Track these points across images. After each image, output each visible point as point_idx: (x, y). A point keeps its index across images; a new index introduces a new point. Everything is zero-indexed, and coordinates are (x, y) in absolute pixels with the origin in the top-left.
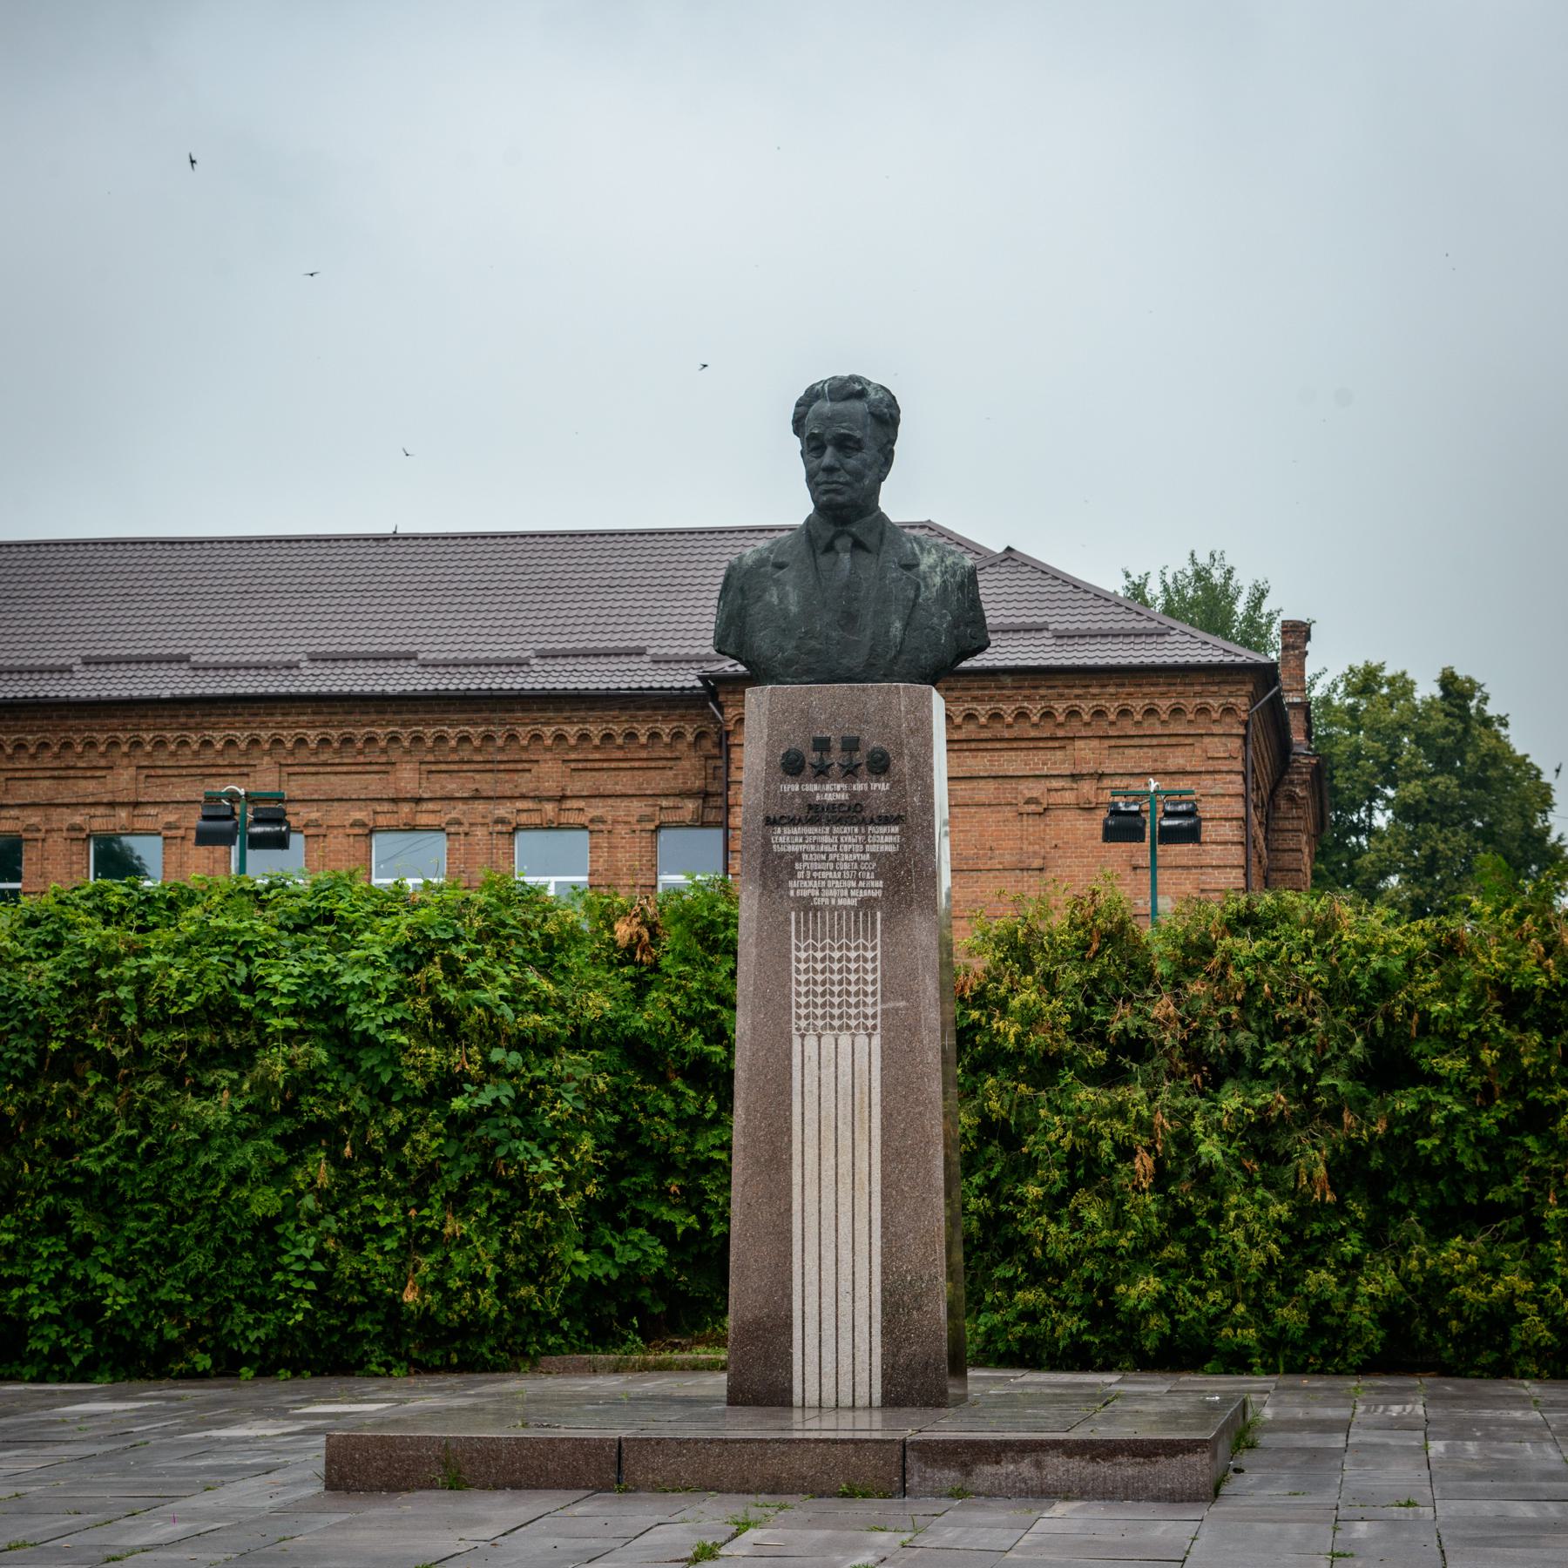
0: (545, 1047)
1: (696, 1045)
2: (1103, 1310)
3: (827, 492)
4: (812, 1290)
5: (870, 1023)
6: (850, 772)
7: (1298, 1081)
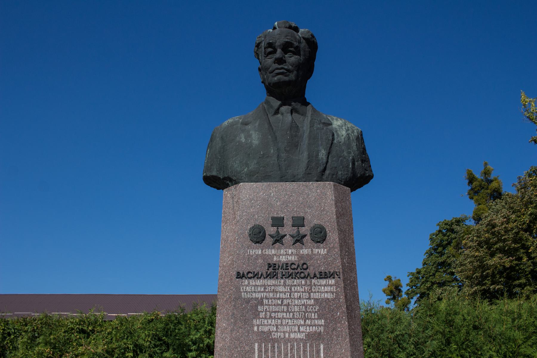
3: (278, 74)
6: (299, 240)
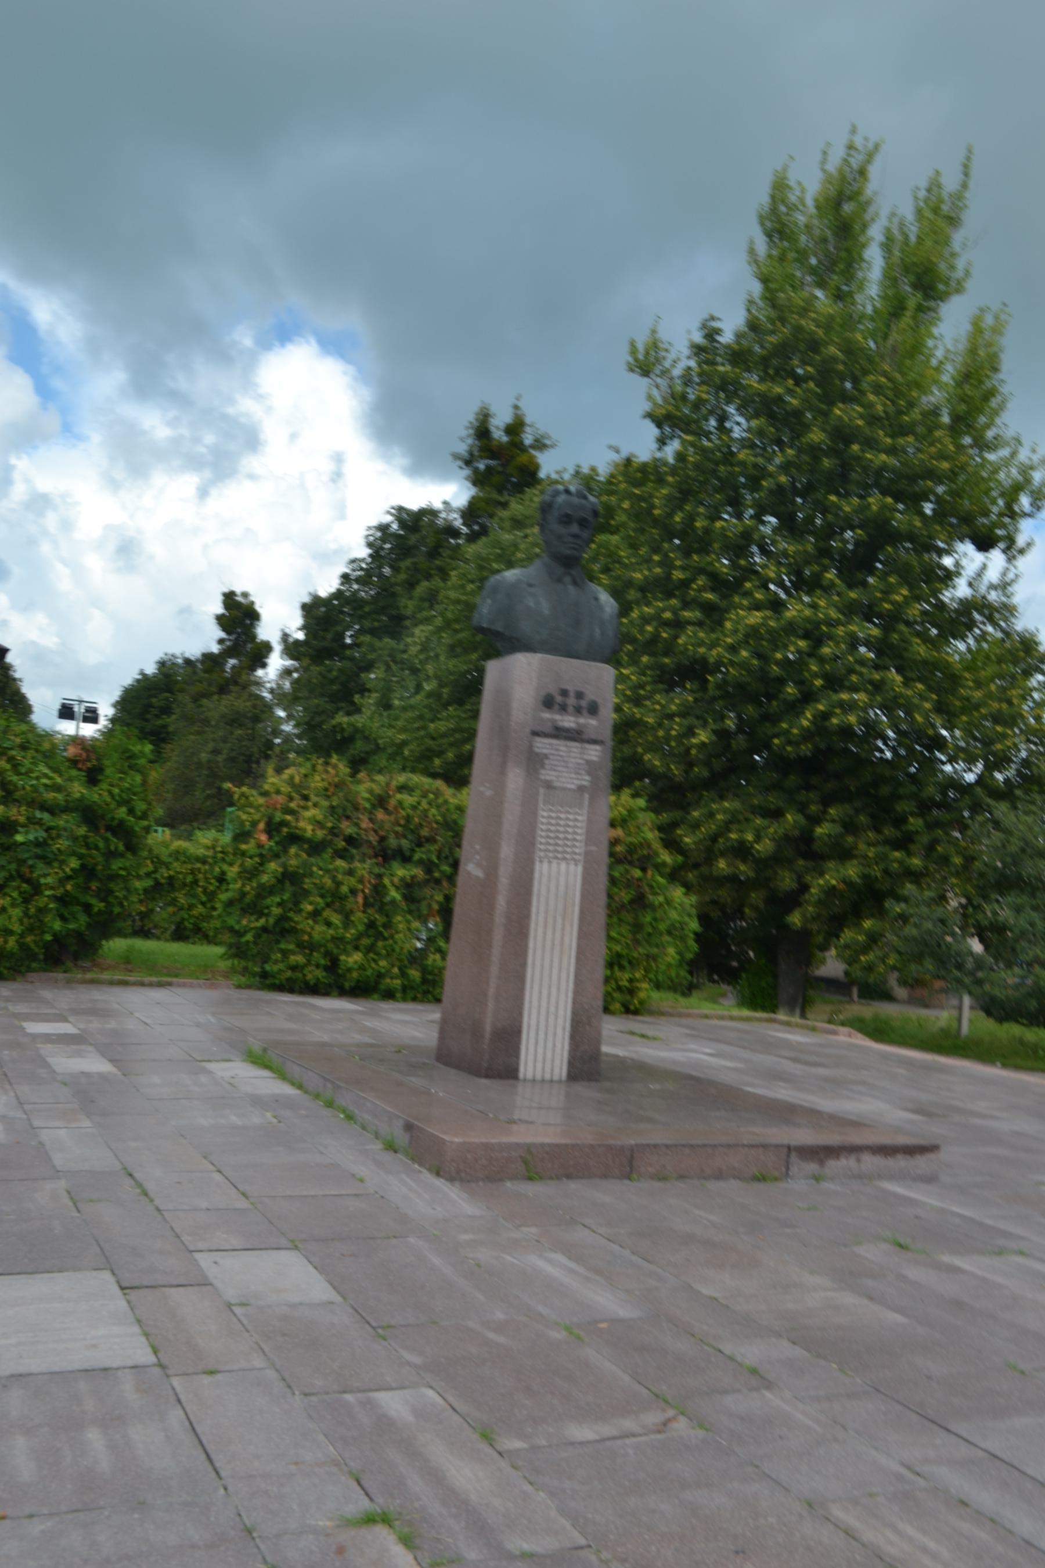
0: (51, 809)
1: (124, 816)
2: (333, 965)
4: (534, 1011)
5: (577, 857)
6: (578, 711)
7: (429, 867)
